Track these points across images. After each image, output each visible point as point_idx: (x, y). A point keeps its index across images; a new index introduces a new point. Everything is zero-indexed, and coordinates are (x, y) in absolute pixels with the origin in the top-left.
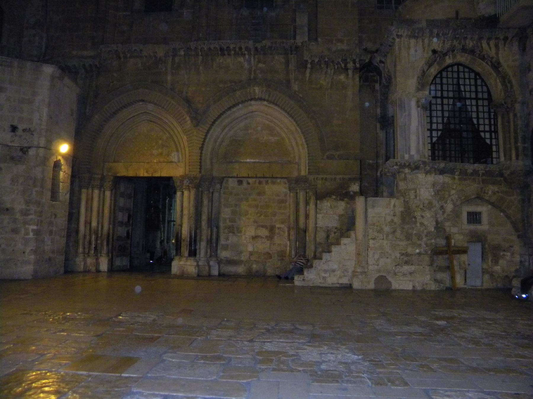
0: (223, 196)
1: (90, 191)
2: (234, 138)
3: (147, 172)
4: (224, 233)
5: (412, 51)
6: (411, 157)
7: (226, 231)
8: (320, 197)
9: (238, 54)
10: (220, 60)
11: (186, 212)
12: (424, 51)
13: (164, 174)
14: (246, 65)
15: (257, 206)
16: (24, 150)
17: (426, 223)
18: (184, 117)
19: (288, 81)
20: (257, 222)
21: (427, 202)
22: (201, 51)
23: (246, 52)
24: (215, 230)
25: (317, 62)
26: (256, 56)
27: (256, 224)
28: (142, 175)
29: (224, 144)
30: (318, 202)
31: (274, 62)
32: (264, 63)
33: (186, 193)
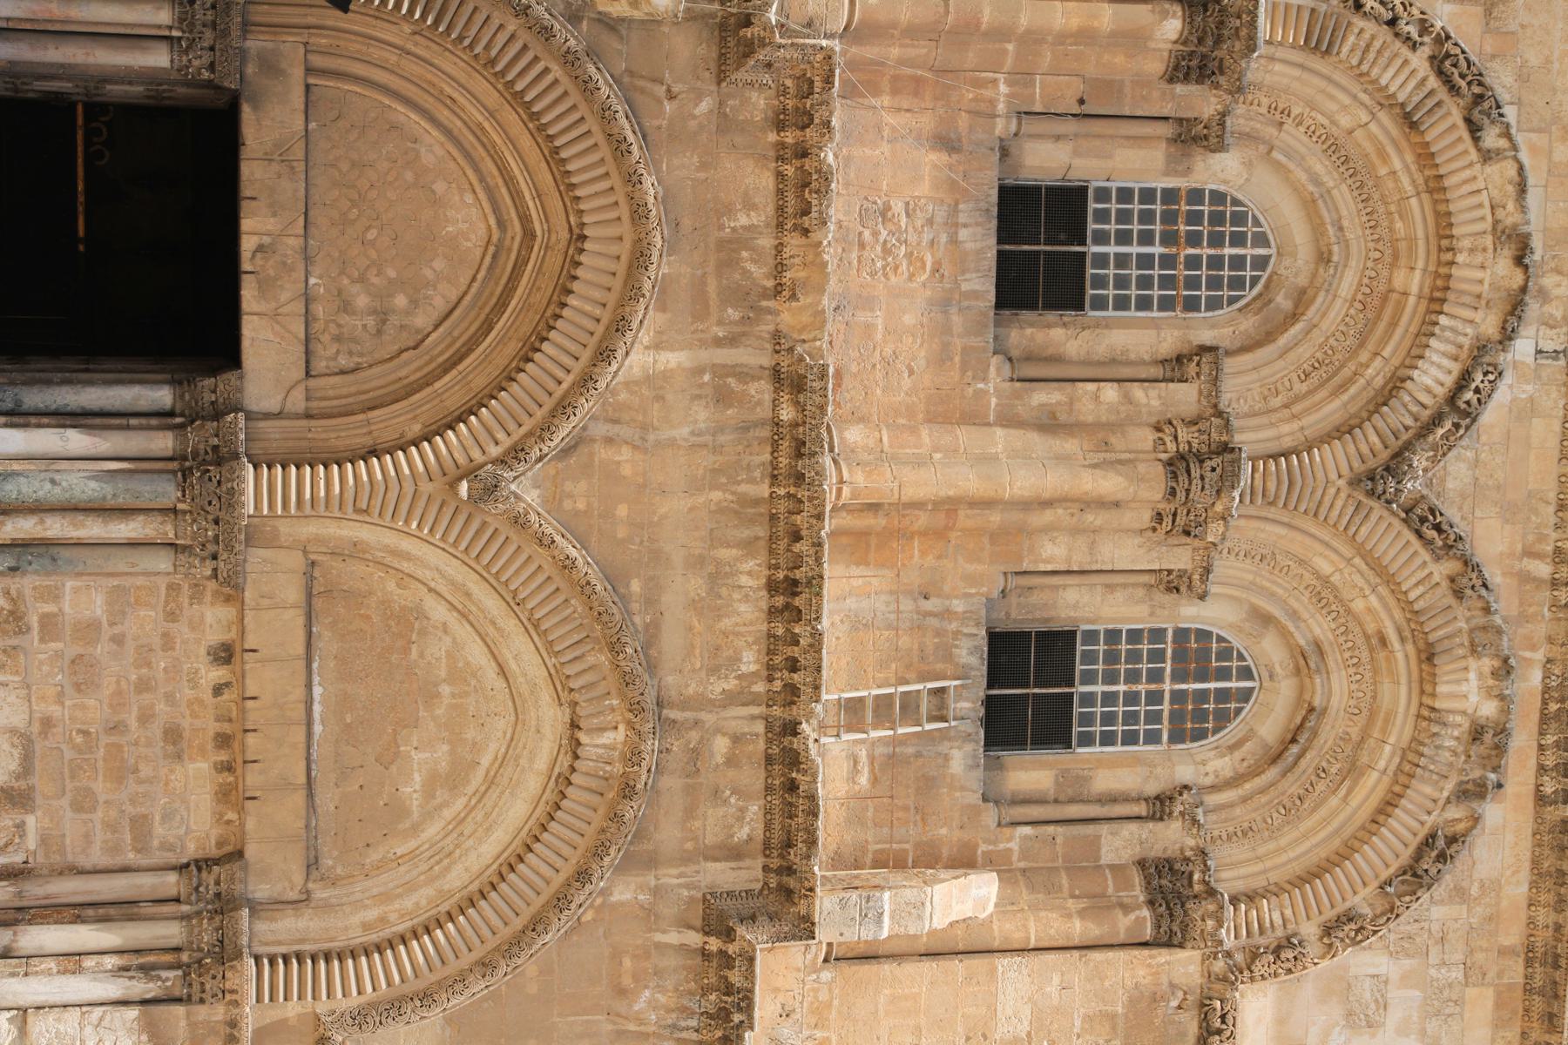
2: (417, 625)
3: (260, 248)
9: (770, 652)
10: (750, 573)
13: (253, 331)
14: (719, 686)
15: (116, 728)
18: (501, 436)
19: (651, 862)
20: (44, 733)
22: (789, 496)
23: (777, 686)
25: (726, 978)
26: (760, 727)
27: (36, 728)
28: (246, 224)
29: (391, 586)
31: (733, 800)
32: (731, 761)
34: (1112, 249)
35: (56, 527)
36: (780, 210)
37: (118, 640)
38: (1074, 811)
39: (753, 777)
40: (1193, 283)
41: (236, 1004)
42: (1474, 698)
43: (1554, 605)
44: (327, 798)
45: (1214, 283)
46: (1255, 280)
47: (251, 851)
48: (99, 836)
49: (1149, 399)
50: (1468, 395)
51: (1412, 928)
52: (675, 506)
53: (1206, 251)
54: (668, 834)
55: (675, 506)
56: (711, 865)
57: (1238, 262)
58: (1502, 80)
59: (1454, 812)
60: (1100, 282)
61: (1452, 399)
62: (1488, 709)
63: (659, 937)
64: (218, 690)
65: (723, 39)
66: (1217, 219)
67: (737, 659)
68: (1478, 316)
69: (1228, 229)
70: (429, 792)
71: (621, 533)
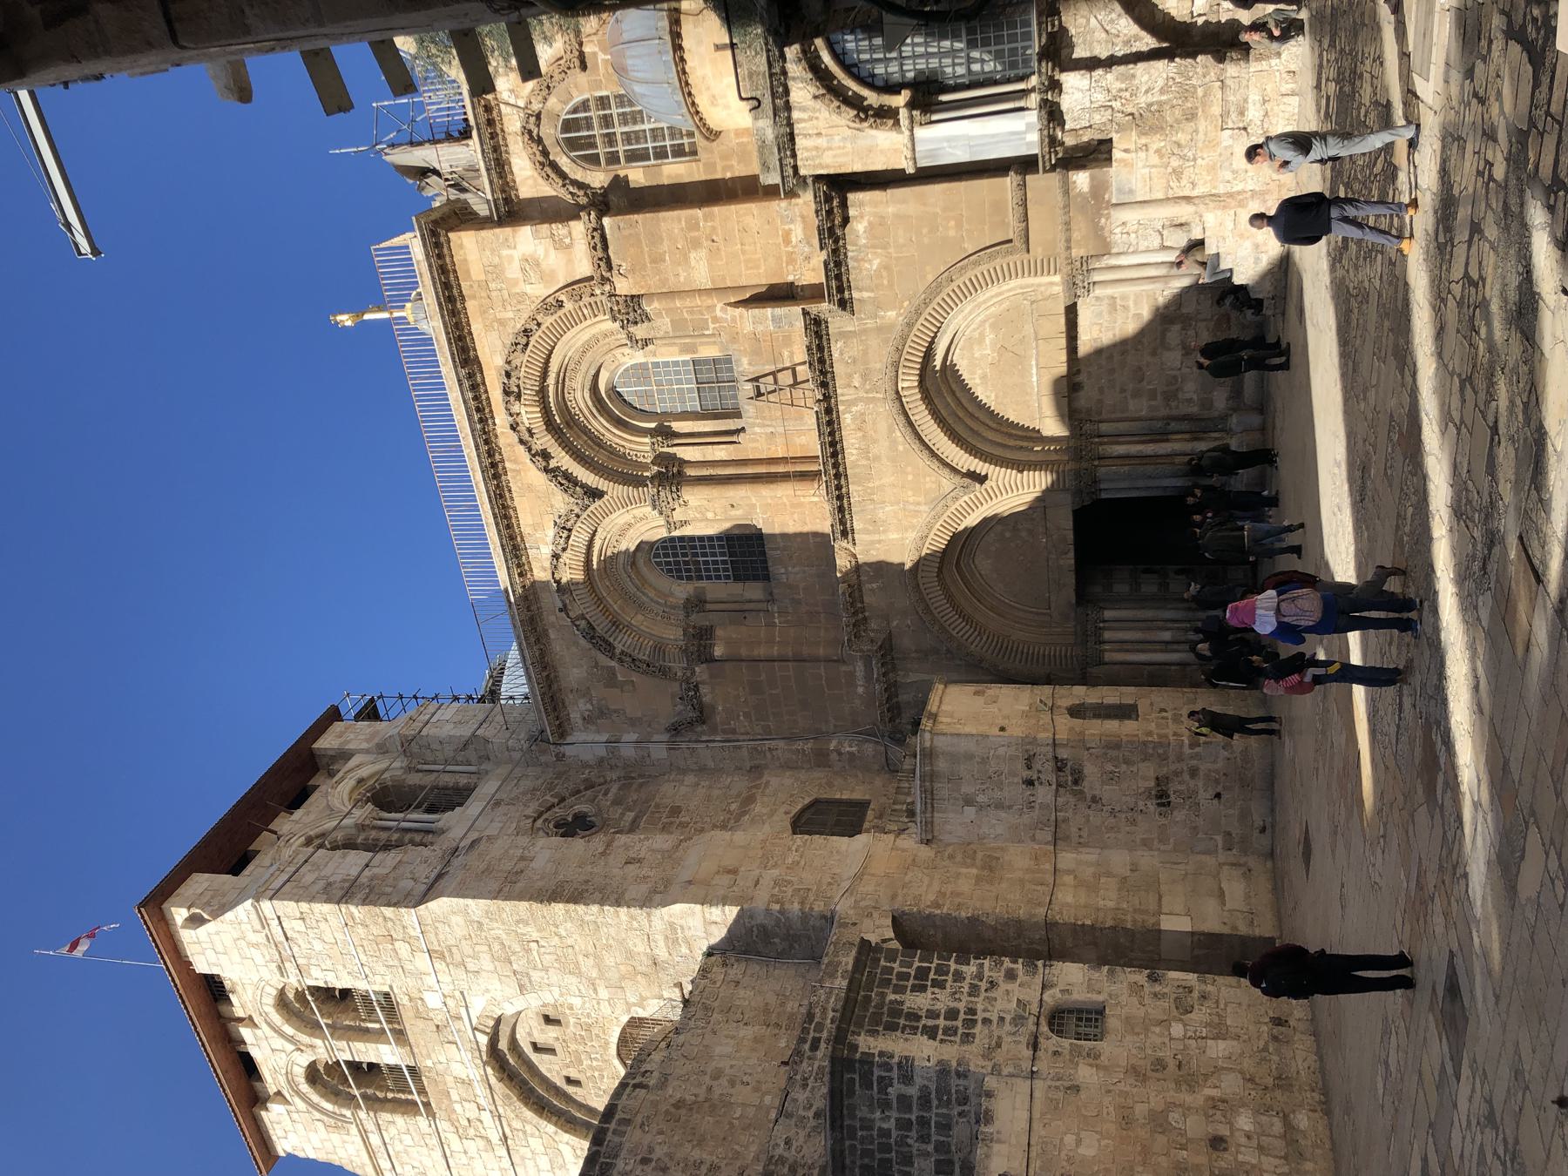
0: (1104, 416)
1: (1107, 647)
4: (1177, 407)
5: (821, 142)
6: (1029, 127)
7: (1173, 404)
8: (1105, 249)
11: (1140, 484)
12: (817, 118)
14: (859, 407)
16: (1060, 765)
17: (1161, 83)
19: (880, 329)
21: (1118, 85)
24: (1173, 425)
26: (839, 391)
28: (1073, 562)
30: (1114, 250)
32: (850, 376)
33: (1102, 486)
34: (719, 559)
35: (1150, 449)
36: (860, 590)
37: (1123, 391)
38: (687, 340)
39: (839, 369)
40: (683, 547)
41: (1067, 258)
42: (523, 412)
43: (500, 454)
44: (1028, 329)
45: (674, 548)
46: (657, 549)
47: (1062, 310)
48: (1131, 304)
49: (691, 514)
50: (564, 535)
51: (519, 307)
52: (888, 480)
53: (680, 559)
54: (874, 342)
55: (888, 480)
56: (852, 329)
57: (667, 555)
58: (583, 642)
59: (516, 362)
60: (721, 547)
61: (570, 530)
62: (516, 408)
63: (872, 295)
64: (1079, 372)
65: (891, 646)
66: (679, 571)
67: (854, 419)
68: (568, 561)
69: (673, 567)
70: (982, 336)
71: (909, 469)
